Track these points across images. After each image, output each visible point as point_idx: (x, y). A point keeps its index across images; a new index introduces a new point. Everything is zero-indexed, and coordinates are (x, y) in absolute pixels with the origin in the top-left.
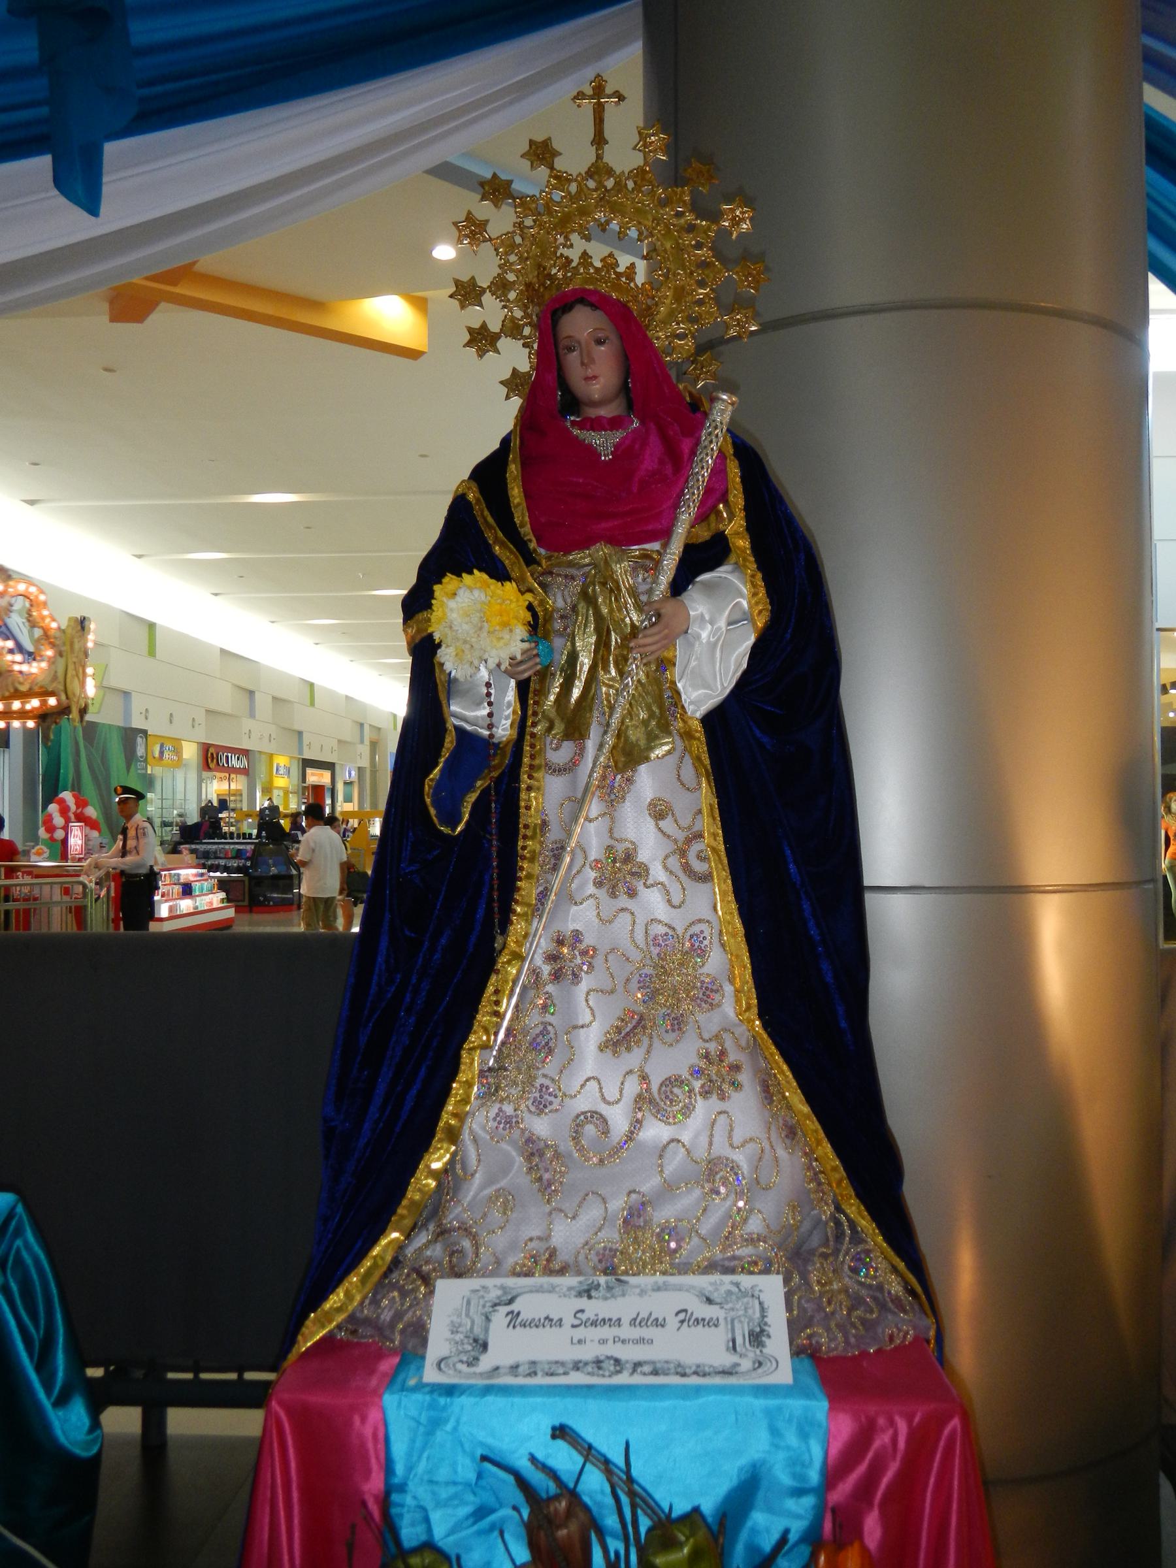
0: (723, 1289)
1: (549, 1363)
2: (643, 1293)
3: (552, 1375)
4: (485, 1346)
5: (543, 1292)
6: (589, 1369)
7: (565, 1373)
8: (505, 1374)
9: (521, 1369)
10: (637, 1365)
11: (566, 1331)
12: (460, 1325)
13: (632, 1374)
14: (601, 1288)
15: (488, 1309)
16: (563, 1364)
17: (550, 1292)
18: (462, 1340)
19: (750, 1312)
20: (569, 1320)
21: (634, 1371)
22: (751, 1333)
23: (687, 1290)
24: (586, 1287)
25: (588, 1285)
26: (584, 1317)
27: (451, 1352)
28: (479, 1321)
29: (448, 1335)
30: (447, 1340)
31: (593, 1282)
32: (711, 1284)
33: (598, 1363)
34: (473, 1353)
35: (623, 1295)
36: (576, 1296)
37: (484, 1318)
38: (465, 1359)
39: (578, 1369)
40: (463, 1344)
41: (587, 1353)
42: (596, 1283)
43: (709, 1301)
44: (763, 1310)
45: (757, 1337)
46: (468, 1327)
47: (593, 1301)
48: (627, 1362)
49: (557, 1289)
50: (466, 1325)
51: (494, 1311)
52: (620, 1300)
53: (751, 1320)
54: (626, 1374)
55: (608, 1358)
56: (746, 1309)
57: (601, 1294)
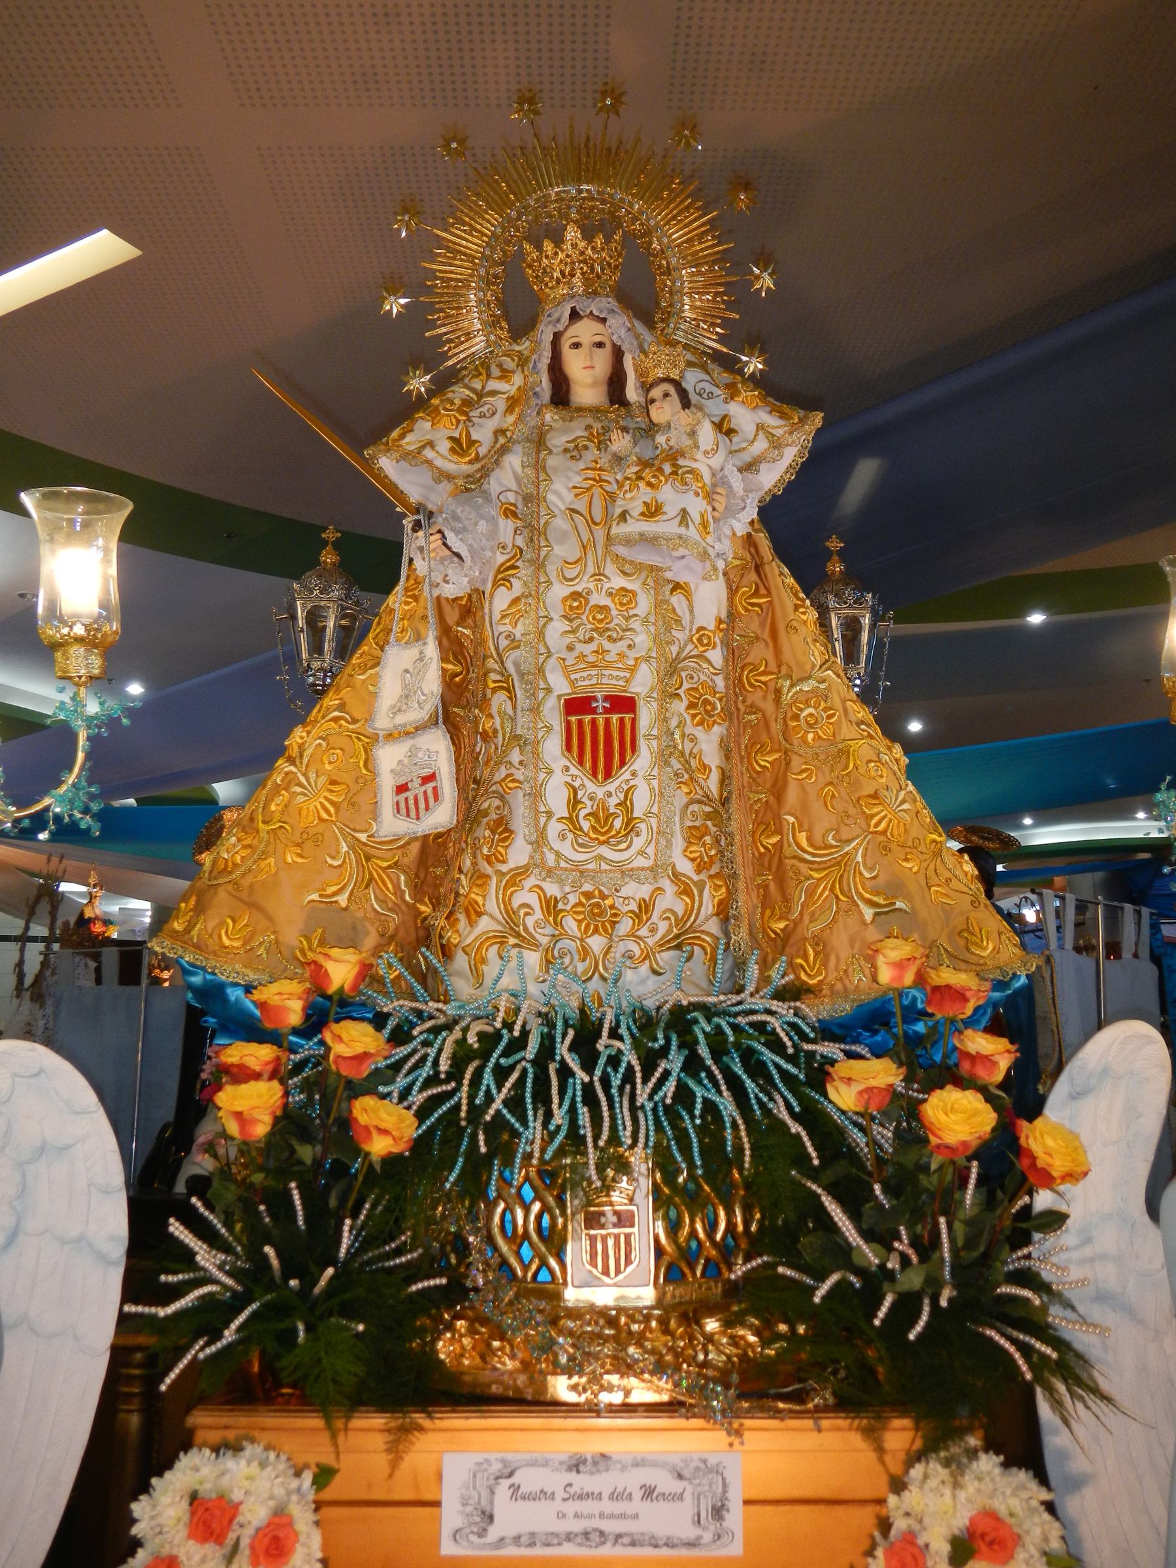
0: (693, 1465)
1: (547, 1534)
2: (624, 1468)
3: (548, 1545)
4: (491, 1518)
6: (579, 1540)
7: (559, 1544)
9: (522, 1539)
10: (619, 1537)
11: (558, 1505)
13: (614, 1545)
15: (492, 1482)
16: (557, 1535)
17: (544, 1466)
19: (714, 1487)
20: (560, 1494)
21: (616, 1541)
22: (713, 1508)
23: (662, 1467)
26: (572, 1490)
28: (485, 1494)
29: (460, 1508)
32: (682, 1461)
33: (586, 1534)
35: (607, 1470)
38: (475, 1530)
39: (569, 1540)
41: (578, 1526)
43: (680, 1477)
44: (725, 1485)
45: (718, 1512)
48: (610, 1534)
52: (604, 1474)
53: (714, 1495)
54: (609, 1544)
55: (595, 1530)
56: (710, 1485)
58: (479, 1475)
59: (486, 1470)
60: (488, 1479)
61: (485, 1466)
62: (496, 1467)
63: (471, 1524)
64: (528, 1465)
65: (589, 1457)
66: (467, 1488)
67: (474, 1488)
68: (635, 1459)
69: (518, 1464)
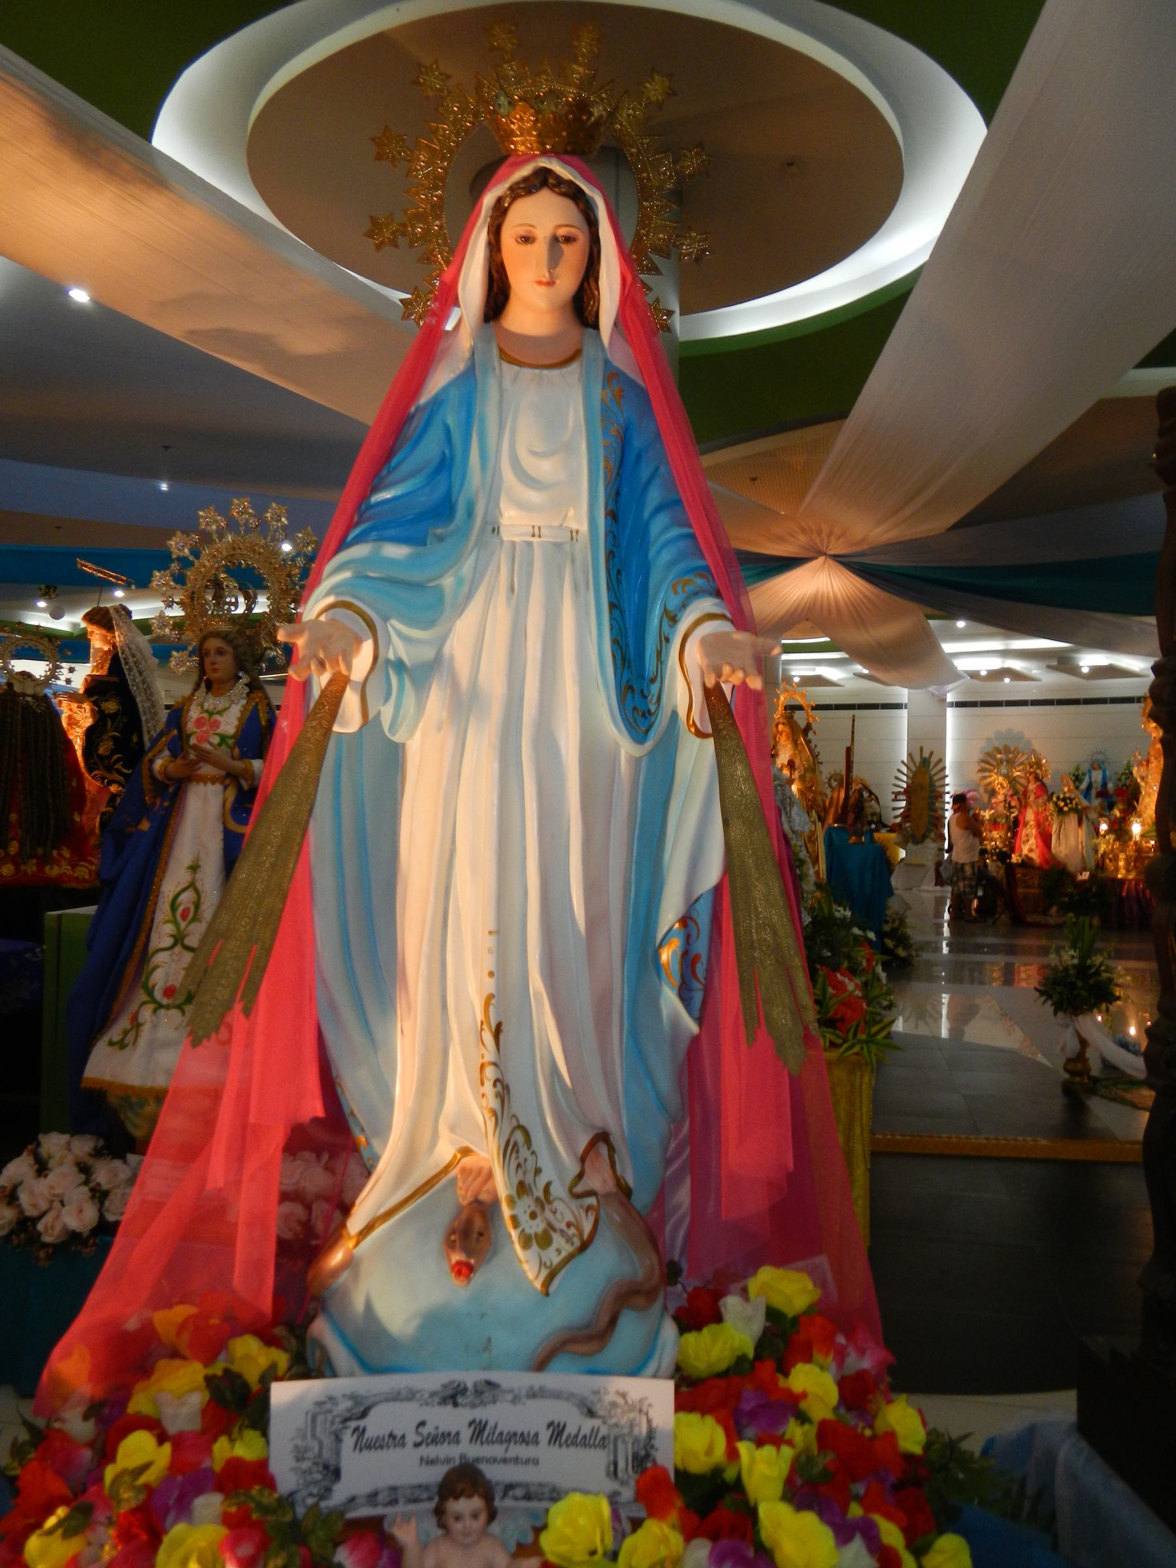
2: (516, 1400)
4: (336, 1474)
5: (402, 1400)
8: (363, 1505)
12: (306, 1450)
14: (468, 1393)
15: (338, 1426)
18: (310, 1469)
24: (450, 1392)
25: (453, 1389)
27: (299, 1485)
28: (328, 1441)
30: (293, 1469)
31: (459, 1386)
34: (324, 1484)
35: (494, 1402)
36: (440, 1404)
37: (333, 1438)
38: (315, 1491)
40: (311, 1473)
42: (462, 1386)
46: (316, 1449)
47: (460, 1410)
49: (418, 1395)
50: (313, 1448)
51: (346, 1428)
52: (490, 1407)
57: (468, 1400)
58: (320, 1419)
59: (330, 1411)
60: (332, 1423)
61: (328, 1406)
62: (344, 1405)
63: (308, 1484)
64: (387, 1400)
65: (470, 1385)
66: (304, 1437)
67: (314, 1436)
68: (531, 1388)
69: (371, 1400)
